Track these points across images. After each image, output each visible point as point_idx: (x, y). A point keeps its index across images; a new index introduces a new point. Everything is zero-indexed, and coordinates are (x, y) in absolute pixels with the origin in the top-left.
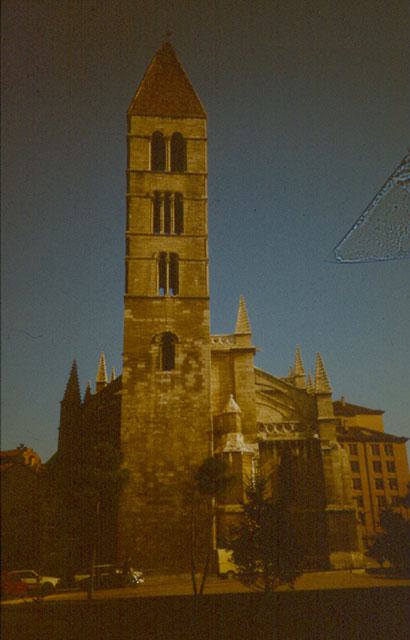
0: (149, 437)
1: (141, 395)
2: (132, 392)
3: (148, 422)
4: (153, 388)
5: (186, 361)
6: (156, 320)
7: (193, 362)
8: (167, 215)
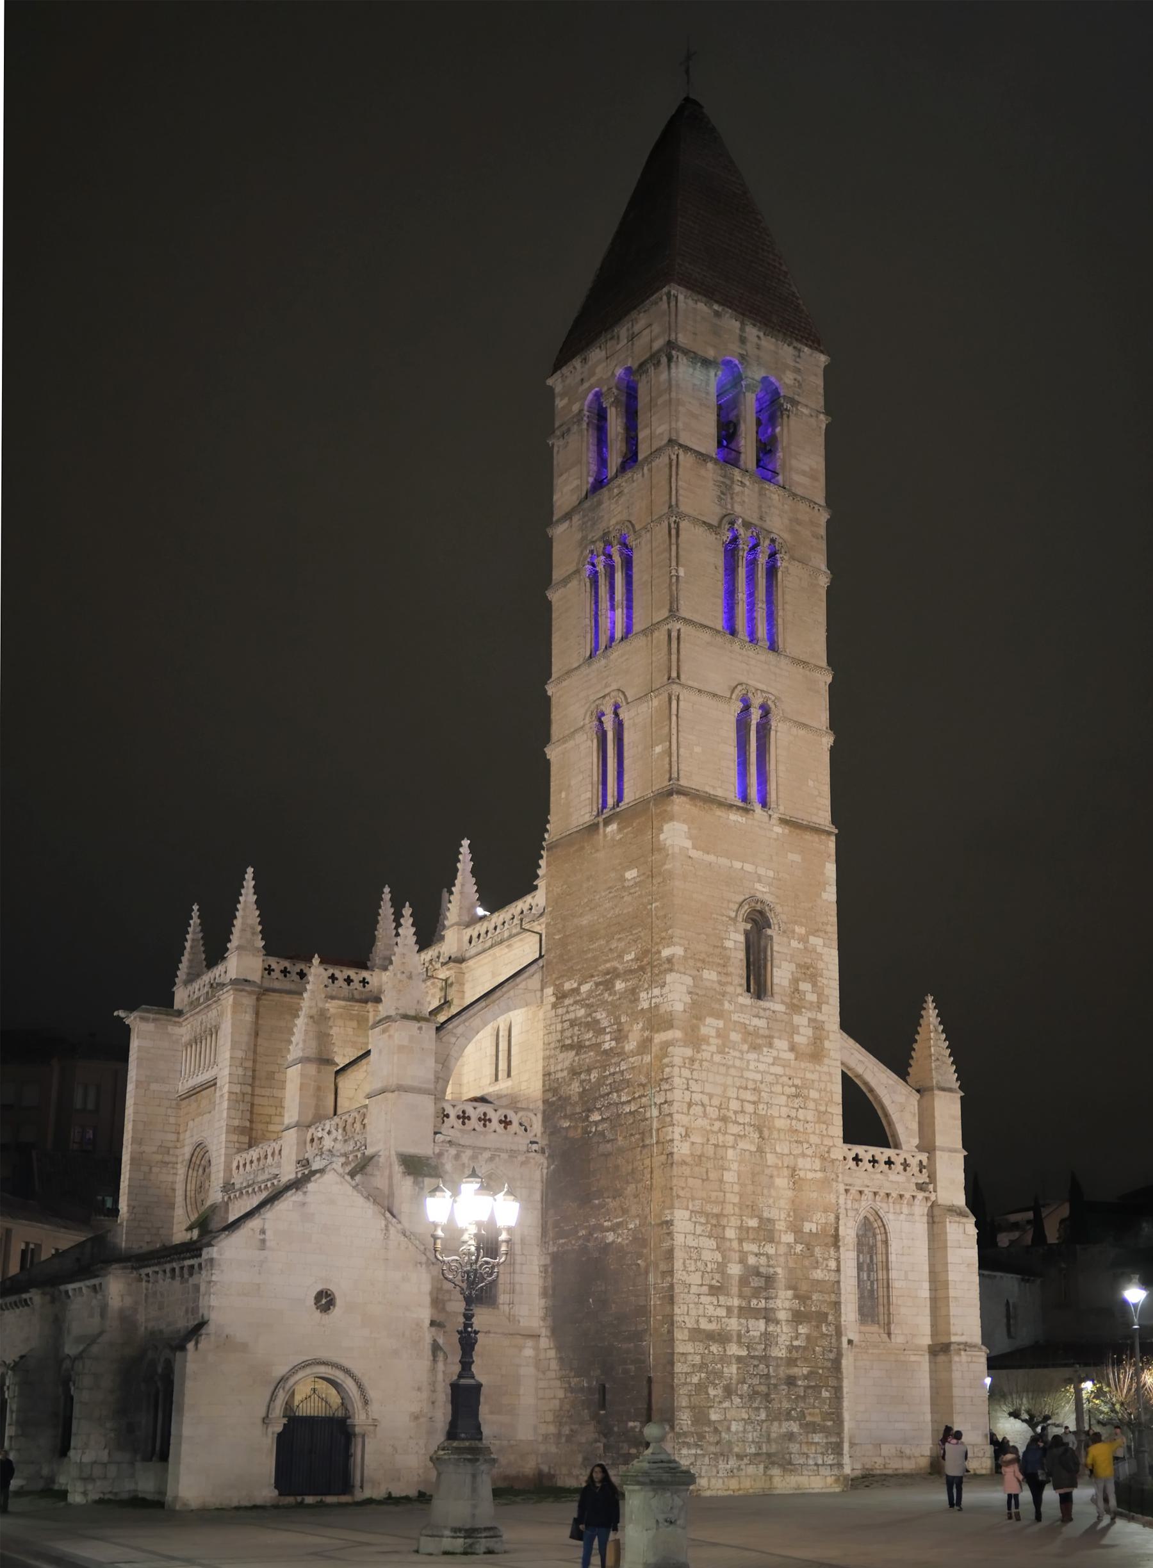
0: (730, 1153)
1: (709, 1050)
2: (695, 1040)
3: (724, 1119)
4: (735, 1037)
5: (795, 981)
6: (738, 865)
7: (805, 986)
8: (751, 595)
